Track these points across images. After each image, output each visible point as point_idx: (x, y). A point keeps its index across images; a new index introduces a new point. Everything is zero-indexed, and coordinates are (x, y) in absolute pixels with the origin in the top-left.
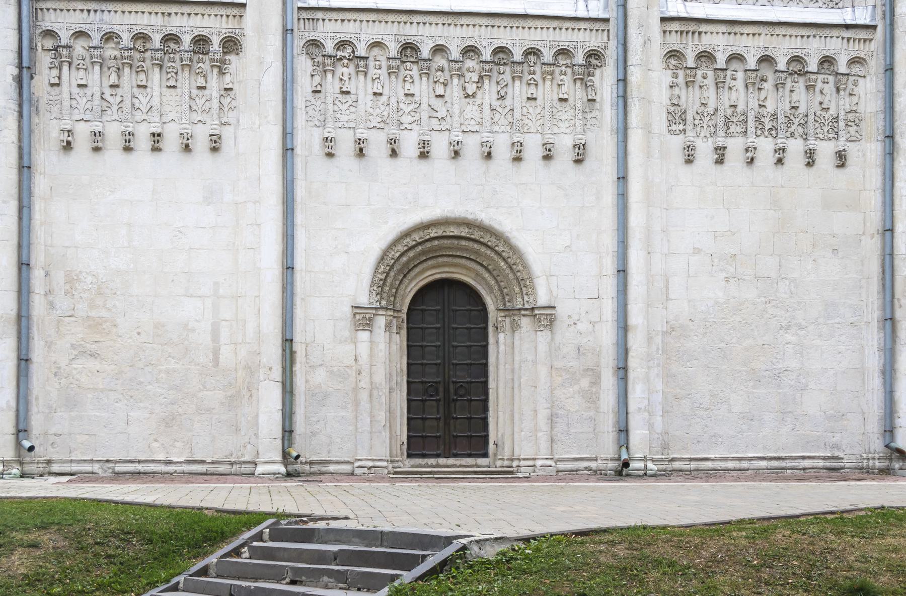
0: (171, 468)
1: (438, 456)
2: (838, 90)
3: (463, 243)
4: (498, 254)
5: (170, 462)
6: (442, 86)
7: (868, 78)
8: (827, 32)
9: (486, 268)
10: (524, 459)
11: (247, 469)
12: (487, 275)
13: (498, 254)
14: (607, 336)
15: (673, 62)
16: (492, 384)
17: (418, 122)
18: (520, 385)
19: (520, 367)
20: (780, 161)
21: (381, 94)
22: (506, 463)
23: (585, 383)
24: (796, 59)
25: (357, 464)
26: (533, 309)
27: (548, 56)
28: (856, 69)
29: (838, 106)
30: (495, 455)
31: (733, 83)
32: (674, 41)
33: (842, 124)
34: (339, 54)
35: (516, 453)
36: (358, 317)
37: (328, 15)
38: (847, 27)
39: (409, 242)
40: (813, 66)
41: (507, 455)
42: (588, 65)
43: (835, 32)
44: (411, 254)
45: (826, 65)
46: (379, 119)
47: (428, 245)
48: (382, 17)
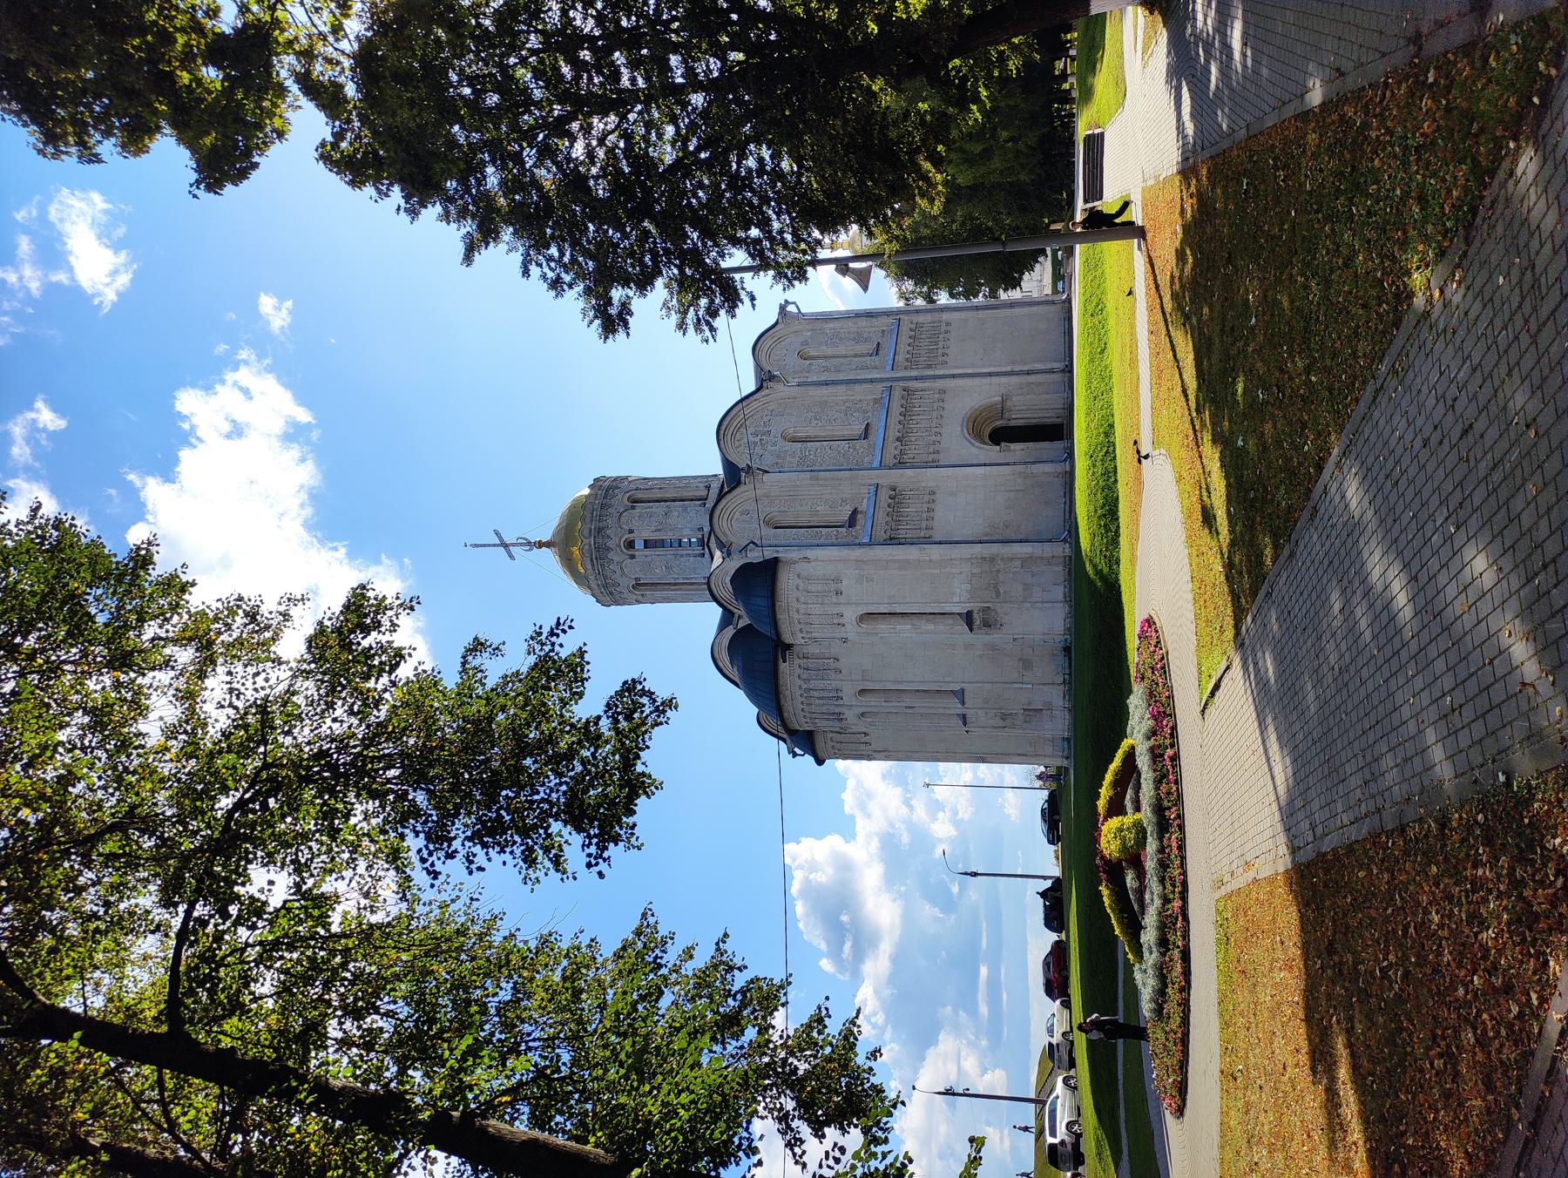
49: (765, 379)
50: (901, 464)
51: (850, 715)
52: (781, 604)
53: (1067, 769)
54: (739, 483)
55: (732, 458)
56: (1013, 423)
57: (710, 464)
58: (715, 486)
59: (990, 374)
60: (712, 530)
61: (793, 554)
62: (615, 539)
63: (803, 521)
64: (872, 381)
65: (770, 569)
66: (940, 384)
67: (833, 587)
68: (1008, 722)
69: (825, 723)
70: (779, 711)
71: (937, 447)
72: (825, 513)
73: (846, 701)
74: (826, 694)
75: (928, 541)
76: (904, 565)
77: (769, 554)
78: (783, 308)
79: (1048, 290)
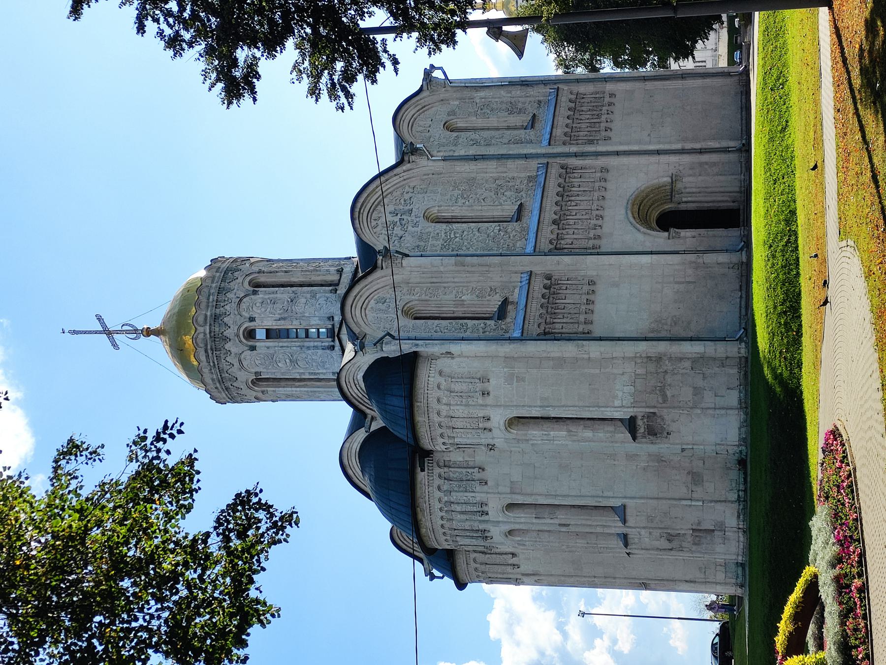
0: (744, 296)
49: (407, 151)
50: (557, 250)
51: (496, 532)
52: (420, 405)
53: (741, 599)
54: (375, 268)
55: (369, 239)
56: (683, 207)
57: (346, 247)
58: (348, 270)
59: (658, 152)
60: (344, 319)
61: (435, 349)
62: (234, 325)
63: (449, 308)
64: (526, 157)
65: (409, 364)
66: (601, 162)
67: (479, 386)
68: (675, 544)
69: (467, 541)
70: (415, 527)
71: (598, 232)
72: (470, 301)
73: (492, 516)
74: (469, 508)
75: (588, 337)
76: (560, 363)
77: (408, 347)
78: (428, 73)
79: (723, 63)
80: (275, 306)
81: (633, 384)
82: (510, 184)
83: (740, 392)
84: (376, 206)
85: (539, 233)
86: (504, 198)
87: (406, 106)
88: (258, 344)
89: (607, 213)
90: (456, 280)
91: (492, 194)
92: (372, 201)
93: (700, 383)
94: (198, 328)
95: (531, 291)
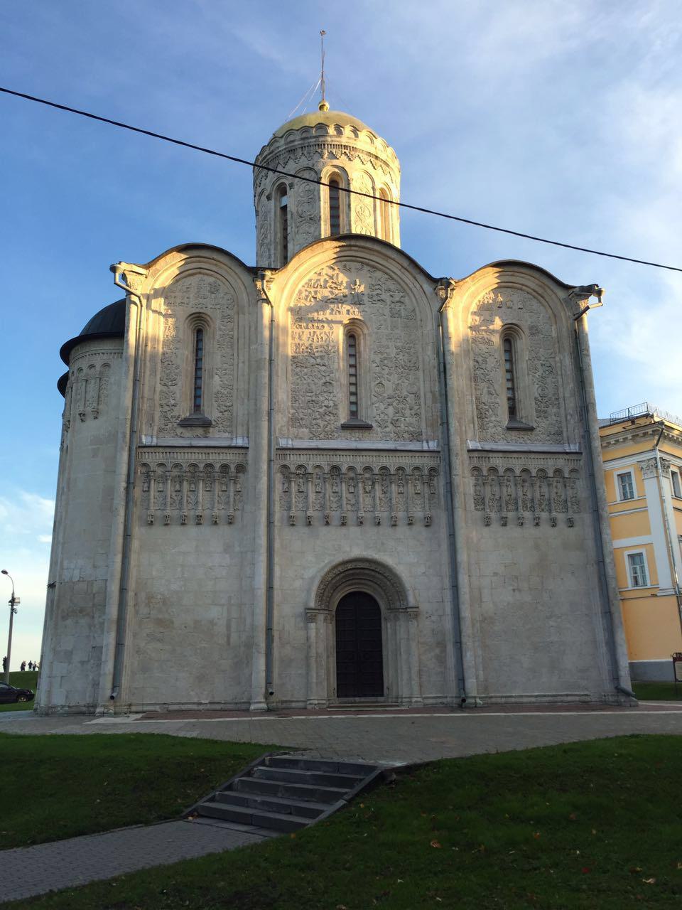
1: (355, 696)
2: (565, 486)
3: (367, 572)
4: (386, 577)
5: (201, 704)
6: (353, 489)
7: (581, 480)
8: (557, 456)
9: (378, 585)
10: (405, 698)
11: (244, 707)
12: (380, 590)
13: (386, 577)
14: (448, 624)
15: (476, 473)
16: (384, 653)
17: (341, 506)
18: (400, 653)
19: (400, 642)
20: (537, 524)
21: (320, 492)
22: (394, 700)
23: (437, 651)
24: (541, 470)
25: (308, 703)
26: (406, 608)
27: (409, 471)
28: (574, 475)
29: (566, 495)
30: (388, 695)
31: (508, 483)
32: (476, 463)
33: (569, 504)
34: (298, 472)
35: (400, 694)
36: (309, 615)
37: (292, 452)
38: (567, 453)
39: (336, 571)
40: (551, 474)
41: (394, 694)
42: (430, 475)
43: (561, 456)
44: (338, 578)
45: (557, 473)
46: (319, 506)
47: (347, 573)
48: (320, 452)
80: (306, 204)
81: (81, 580)
82: (407, 412)
83: (63, 707)
84: (368, 265)
85: (315, 452)
86: (382, 407)
87: (537, 275)
88: (272, 202)
89: (354, 530)
90: (241, 365)
91: (390, 392)
92: (372, 258)
93: (76, 658)
94: (283, 139)
95: (217, 451)
